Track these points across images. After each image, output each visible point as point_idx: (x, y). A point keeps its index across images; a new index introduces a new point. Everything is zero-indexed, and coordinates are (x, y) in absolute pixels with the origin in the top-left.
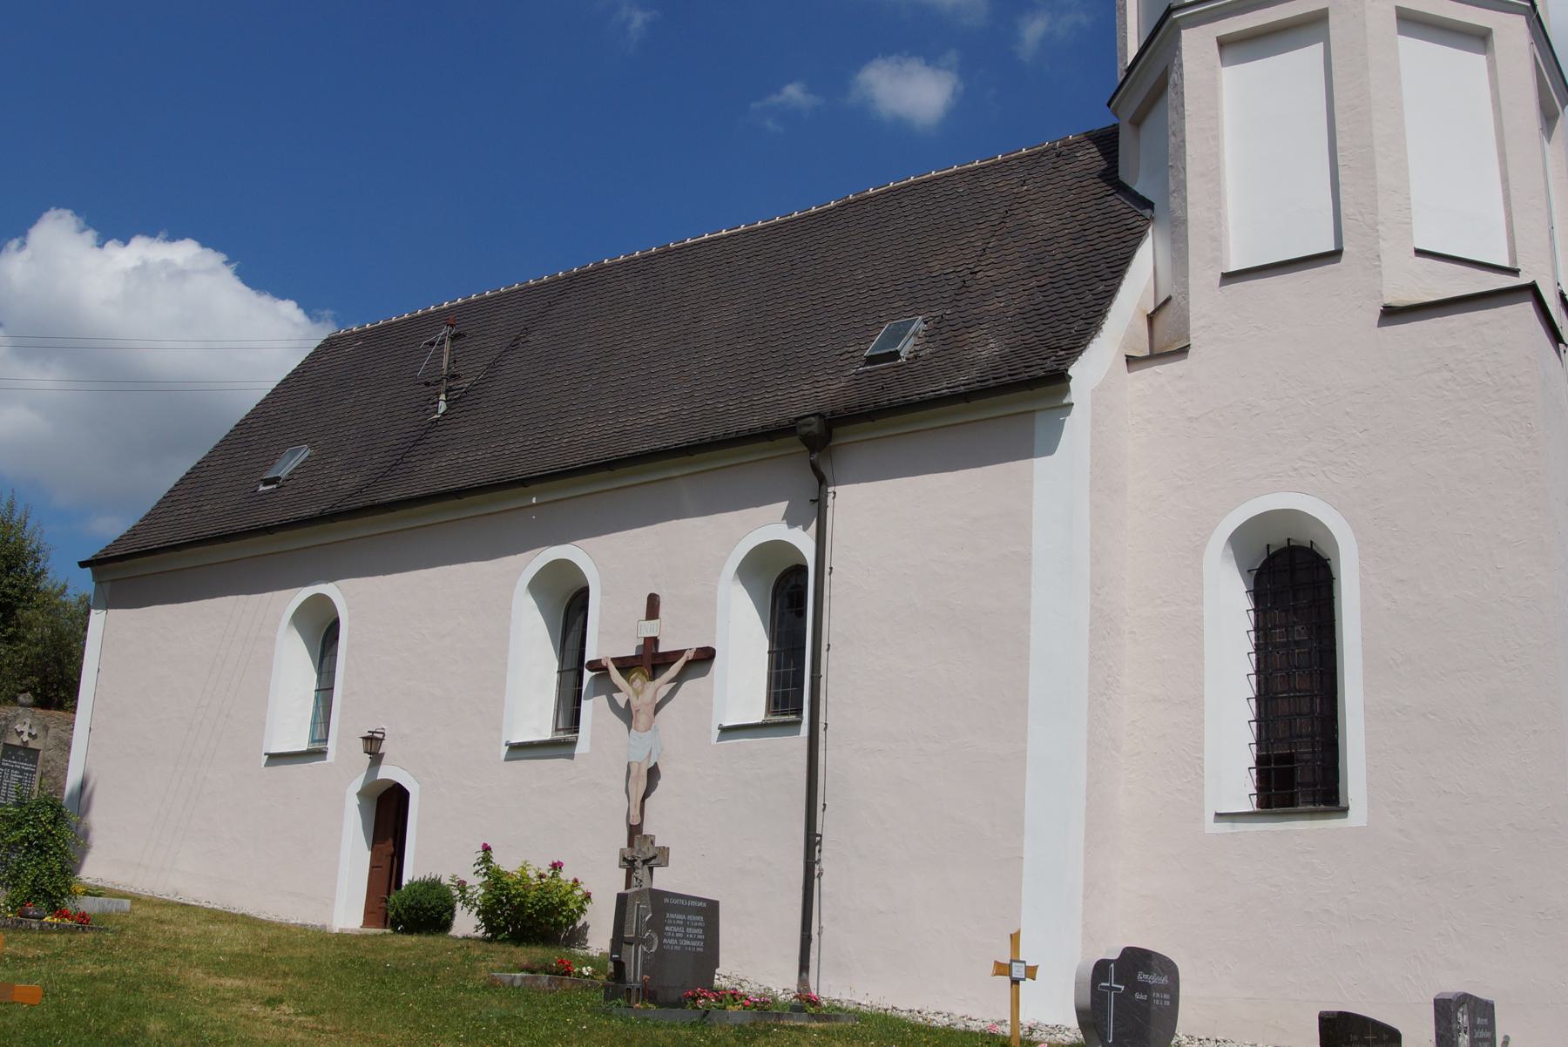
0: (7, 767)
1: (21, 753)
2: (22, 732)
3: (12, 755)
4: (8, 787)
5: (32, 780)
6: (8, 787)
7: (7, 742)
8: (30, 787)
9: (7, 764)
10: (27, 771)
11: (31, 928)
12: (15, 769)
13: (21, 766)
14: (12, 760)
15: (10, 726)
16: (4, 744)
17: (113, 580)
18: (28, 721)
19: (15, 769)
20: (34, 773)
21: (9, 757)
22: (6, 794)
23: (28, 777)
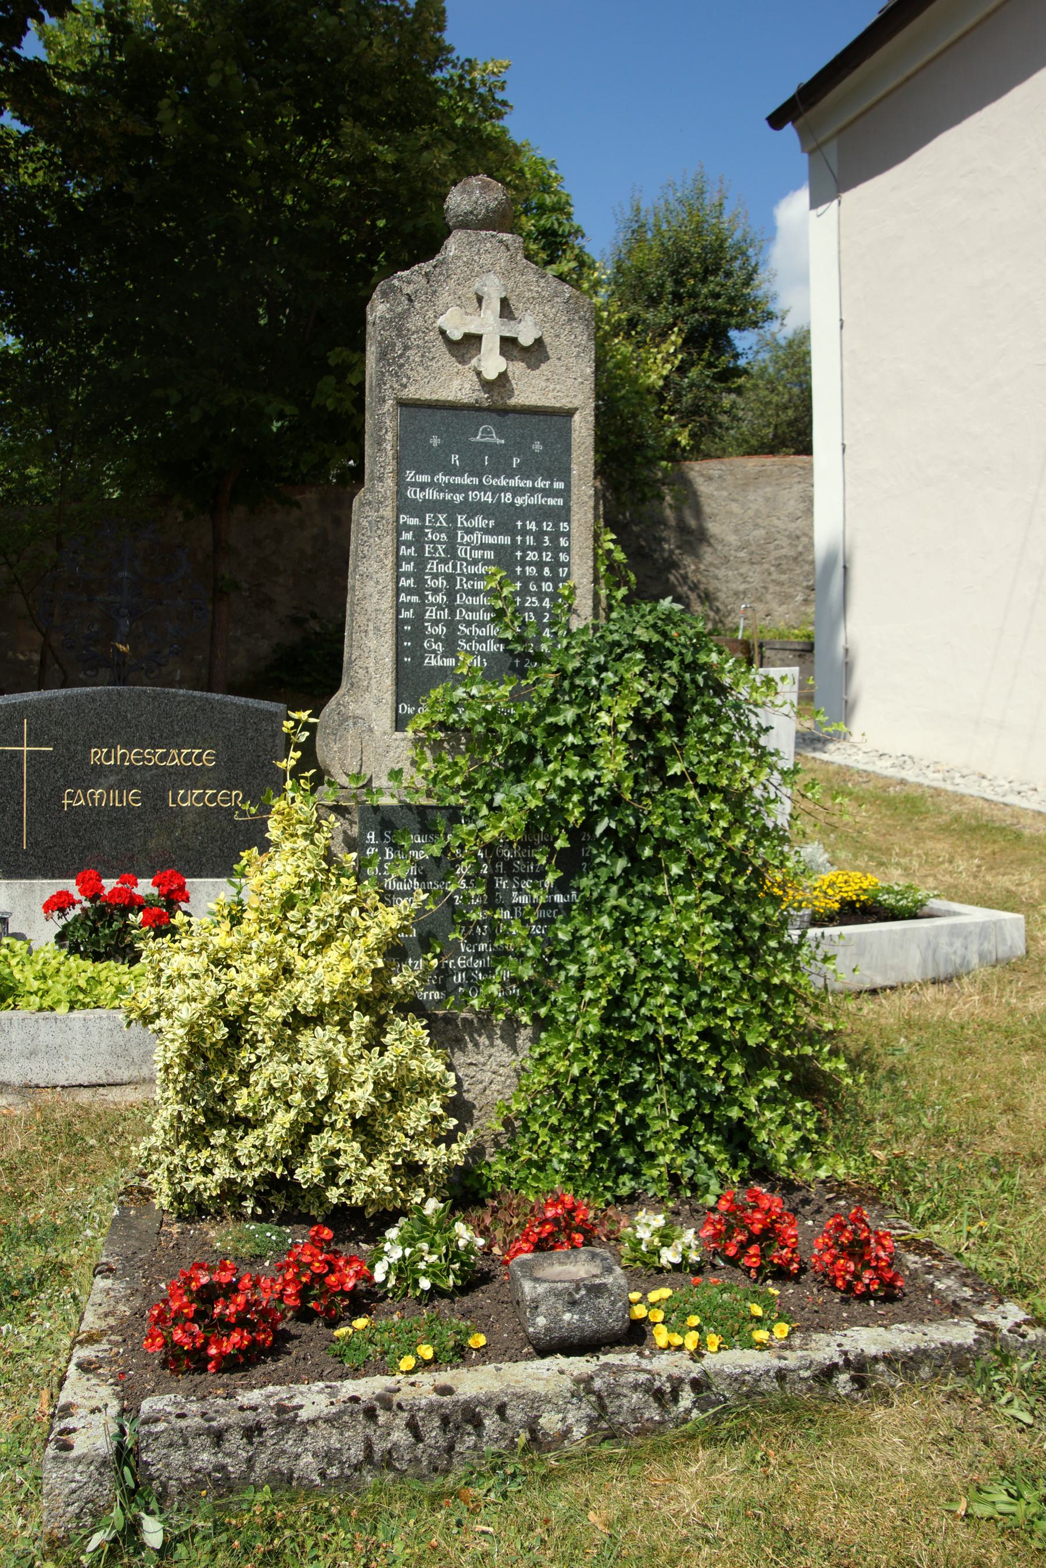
0: (435, 507)
1: (487, 435)
2: (472, 341)
3: (447, 449)
4: (451, 593)
5: (556, 549)
6: (451, 593)
7: (411, 393)
8: (555, 579)
9: (431, 494)
10: (524, 513)
11: (537, 1440)
12: (472, 509)
13: (497, 490)
14: (450, 471)
15: (414, 322)
16: (403, 404)
17: (840, 132)
18: (493, 288)
19: (472, 509)
20: (564, 514)
21: (434, 463)
22: (451, 625)
23: (539, 535)
